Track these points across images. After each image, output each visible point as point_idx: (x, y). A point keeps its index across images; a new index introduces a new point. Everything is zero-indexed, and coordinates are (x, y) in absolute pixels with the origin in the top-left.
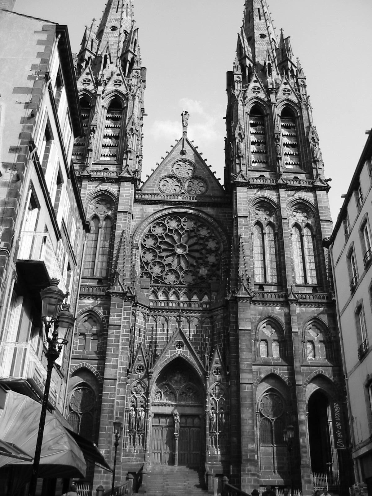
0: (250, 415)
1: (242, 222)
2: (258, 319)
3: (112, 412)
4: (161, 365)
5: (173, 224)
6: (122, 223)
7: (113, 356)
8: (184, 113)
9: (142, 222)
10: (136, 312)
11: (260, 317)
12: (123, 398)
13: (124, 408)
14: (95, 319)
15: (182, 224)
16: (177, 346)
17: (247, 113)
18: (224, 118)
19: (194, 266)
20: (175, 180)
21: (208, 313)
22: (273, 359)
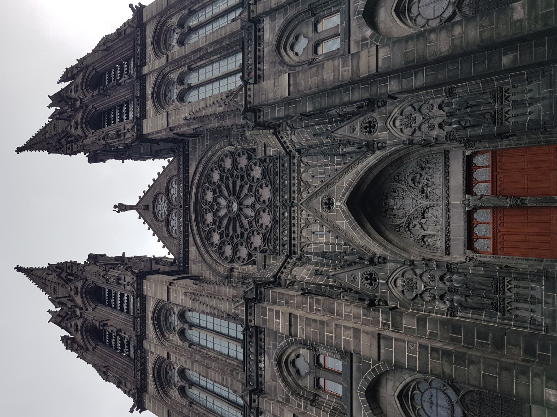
0: (443, 35)
1: (173, 120)
2: (280, 68)
3: (447, 354)
4: (362, 238)
5: (209, 218)
6: (179, 296)
7: (338, 336)
8: (117, 209)
9: (206, 262)
10: (289, 279)
11: (277, 65)
12: (421, 321)
13: (443, 323)
14: (293, 356)
15: (207, 207)
16: (329, 208)
17: (93, 133)
18: (123, 162)
19: (251, 186)
20: (170, 218)
21: (294, 158)
22: (342, 22)
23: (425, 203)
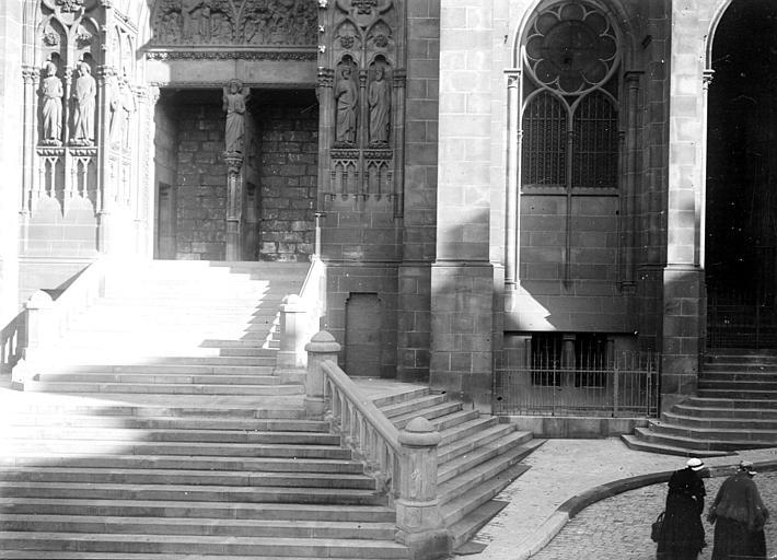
23: (237, 16)
